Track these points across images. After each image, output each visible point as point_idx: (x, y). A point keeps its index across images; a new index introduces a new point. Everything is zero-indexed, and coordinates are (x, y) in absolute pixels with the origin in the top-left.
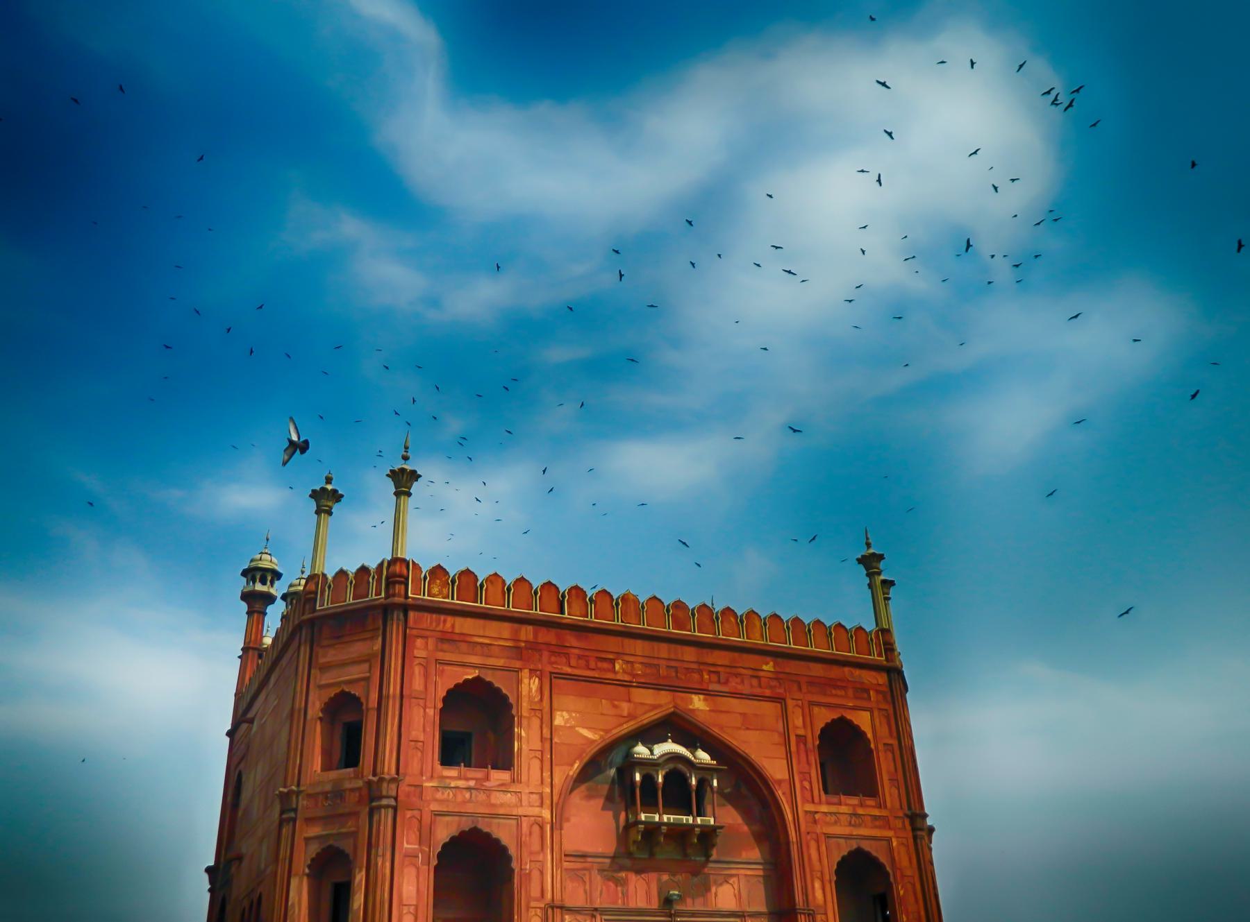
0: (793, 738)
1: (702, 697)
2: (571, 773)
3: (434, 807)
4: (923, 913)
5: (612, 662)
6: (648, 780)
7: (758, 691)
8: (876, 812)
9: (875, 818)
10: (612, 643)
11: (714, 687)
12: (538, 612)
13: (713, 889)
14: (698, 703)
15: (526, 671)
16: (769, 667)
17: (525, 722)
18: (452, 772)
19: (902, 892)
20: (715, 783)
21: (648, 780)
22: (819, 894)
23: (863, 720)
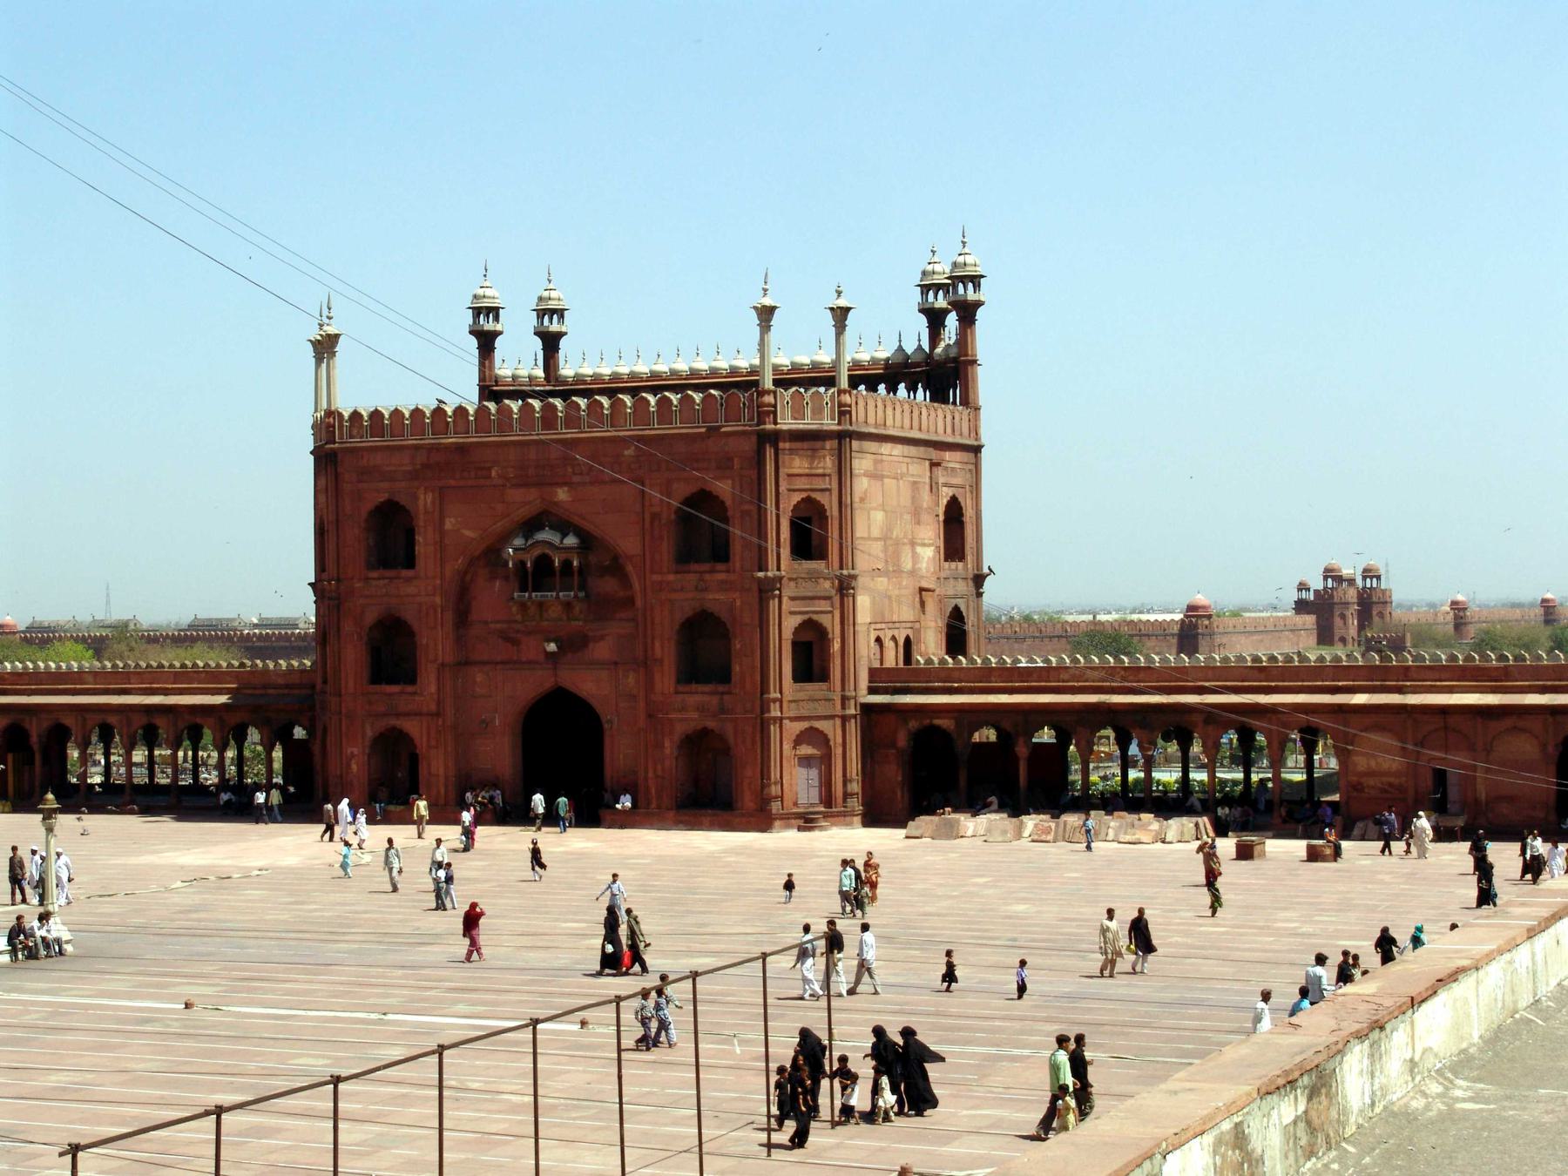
0: (647, 517)
1: (566, 489)
2: (456, 567)
5: (489, 469)
9: (723, 582)
11: (576, 479)
12: (431, 436)
13: (591, 645)
14: (562, 495)
15: (423, 488)
17: (422, 530)
18: (374, 574)
19: (738, 646)
20: (575, 563)
22: (658, 652)
23: (724, 488)
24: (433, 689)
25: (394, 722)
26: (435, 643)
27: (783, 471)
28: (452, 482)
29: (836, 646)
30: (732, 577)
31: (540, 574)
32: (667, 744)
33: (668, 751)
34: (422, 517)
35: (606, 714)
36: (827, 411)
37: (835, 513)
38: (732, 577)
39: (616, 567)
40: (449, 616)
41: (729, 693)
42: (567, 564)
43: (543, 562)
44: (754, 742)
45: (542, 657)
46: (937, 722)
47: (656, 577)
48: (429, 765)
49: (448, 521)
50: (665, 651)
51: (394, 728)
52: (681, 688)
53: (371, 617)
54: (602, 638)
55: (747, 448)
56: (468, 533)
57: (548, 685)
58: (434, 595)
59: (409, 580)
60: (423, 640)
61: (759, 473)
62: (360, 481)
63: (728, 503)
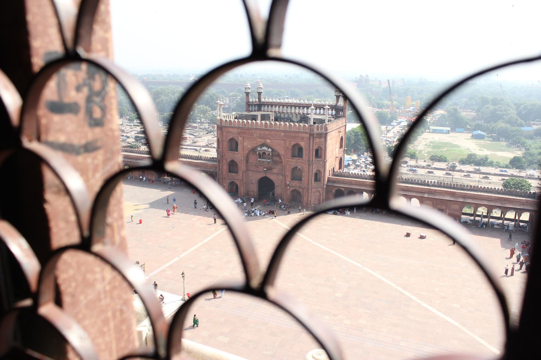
0: (286, 147)
3: (227, 157)
4: (307, 178)
5: (253, 134)
6: (259, 154)
7: (280, 139)
8: (301, 161)
9: (301, 162)
10: (253, 131)
11: (271, 138)
13: (273, 170)
16: (283, 134)
18: (230, 152)
19: (304, 175)
21: (259, 154)
22: (287, 173)
23: (302, 144)
24: (241, 175)
25: (233, 180)
26: (242, 166)
27: (314, 141)
28: (246, 136)
29: (323, 175)
30: (303, 161)
31: (262, 155)
32: (288, 191)
33: (288, 193)
34: (239, 142)
35: (276, 184)
36: (323, 129)
37: (324, 149)
38: (303, 161)
39: (279, 155)
40: (245, 162)
41: (301, 183)
42: (269, 154)
43: (264, 153)
44: (306, 193)
45: (263, 171)
46: (340, 189)
47: (287, 159)
48: (240, 189)
49: (245, 143)
50: (289, 174)
51: (233, 181)
52: (292, 181)
53: (229, 160)
54: (275, 168)
55: (307, 136)
56: (249, 146)
57: (265, 175)
58: (242, 157)
59: (237, 154)
60: (239, 165)
61: (310, 141)
62: (226, 134)
63: (303, 147)
